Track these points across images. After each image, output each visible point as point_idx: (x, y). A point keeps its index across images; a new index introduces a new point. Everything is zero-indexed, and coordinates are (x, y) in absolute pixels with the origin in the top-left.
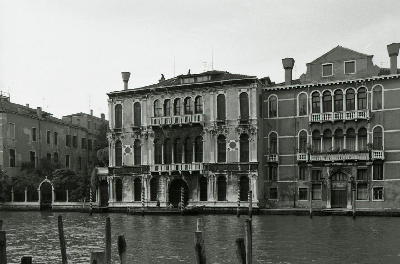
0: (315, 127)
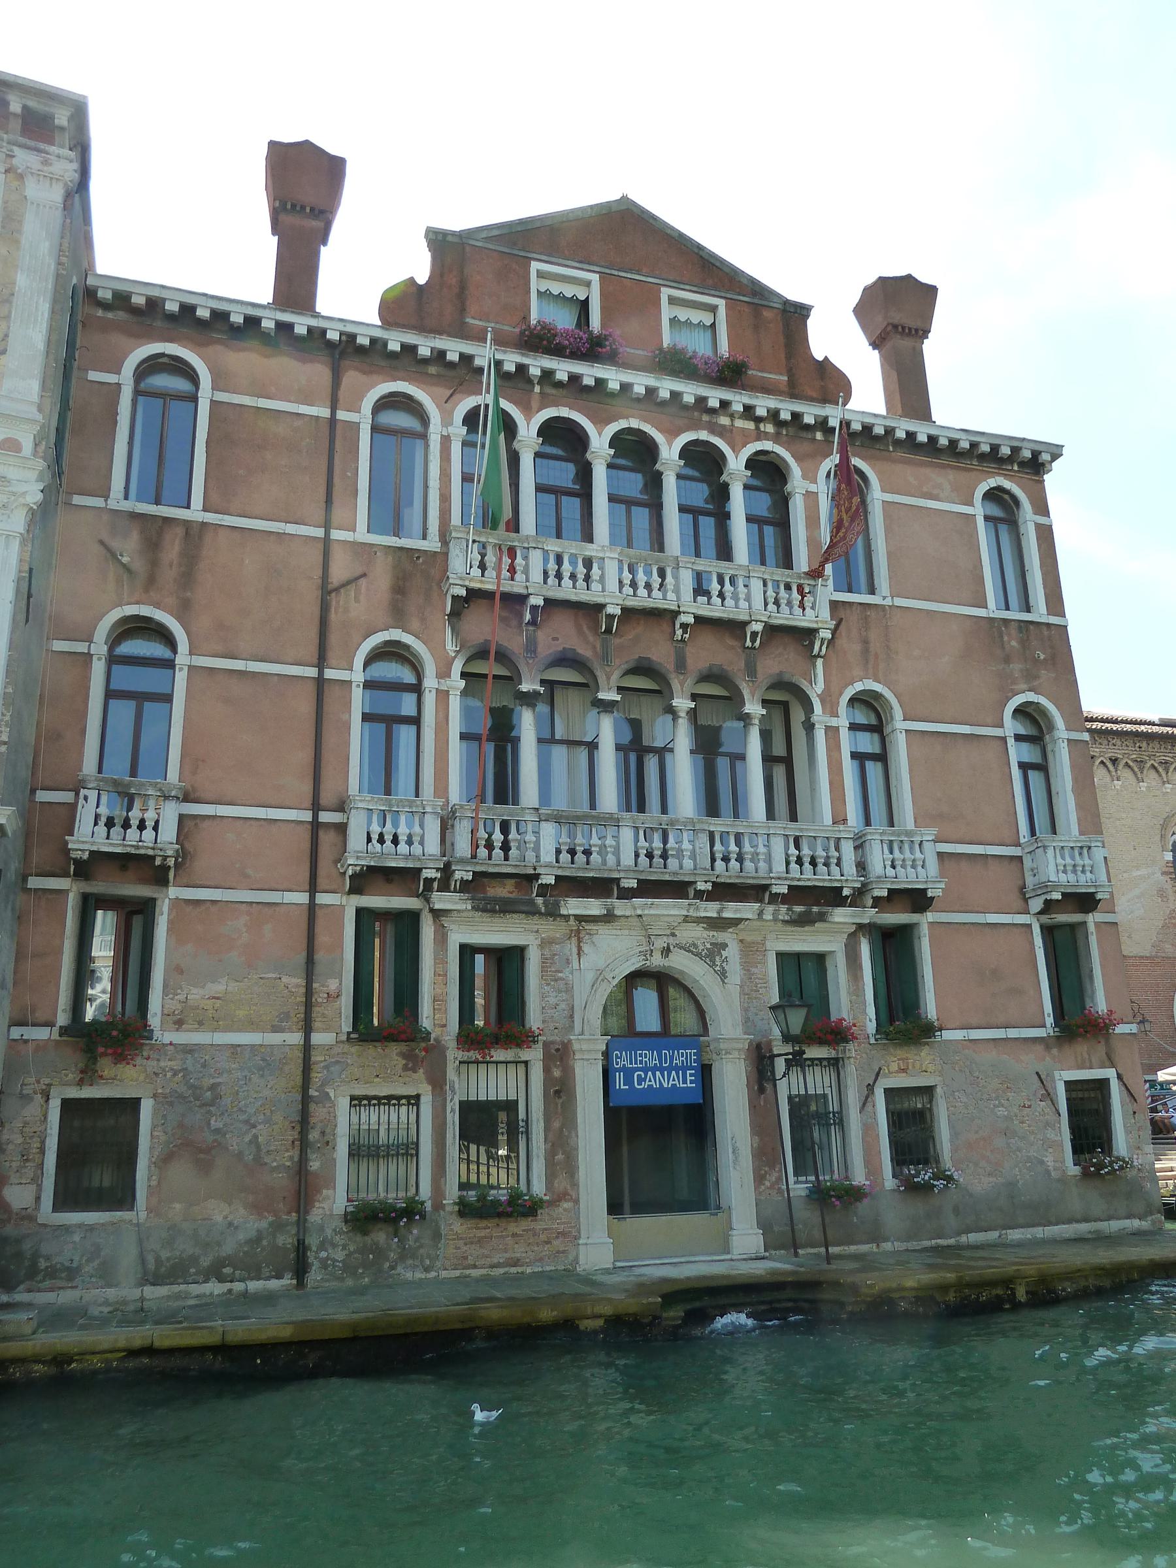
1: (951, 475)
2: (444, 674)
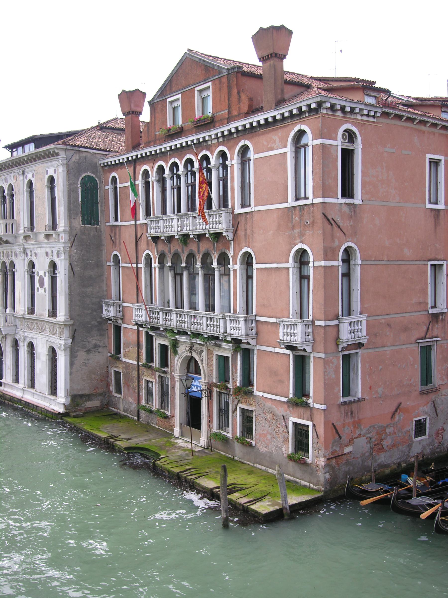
0: (161, 246)
1: (280, 133)
2: (155, 263)
